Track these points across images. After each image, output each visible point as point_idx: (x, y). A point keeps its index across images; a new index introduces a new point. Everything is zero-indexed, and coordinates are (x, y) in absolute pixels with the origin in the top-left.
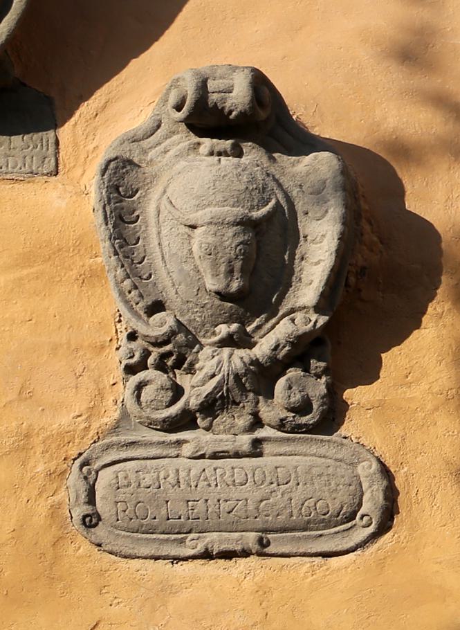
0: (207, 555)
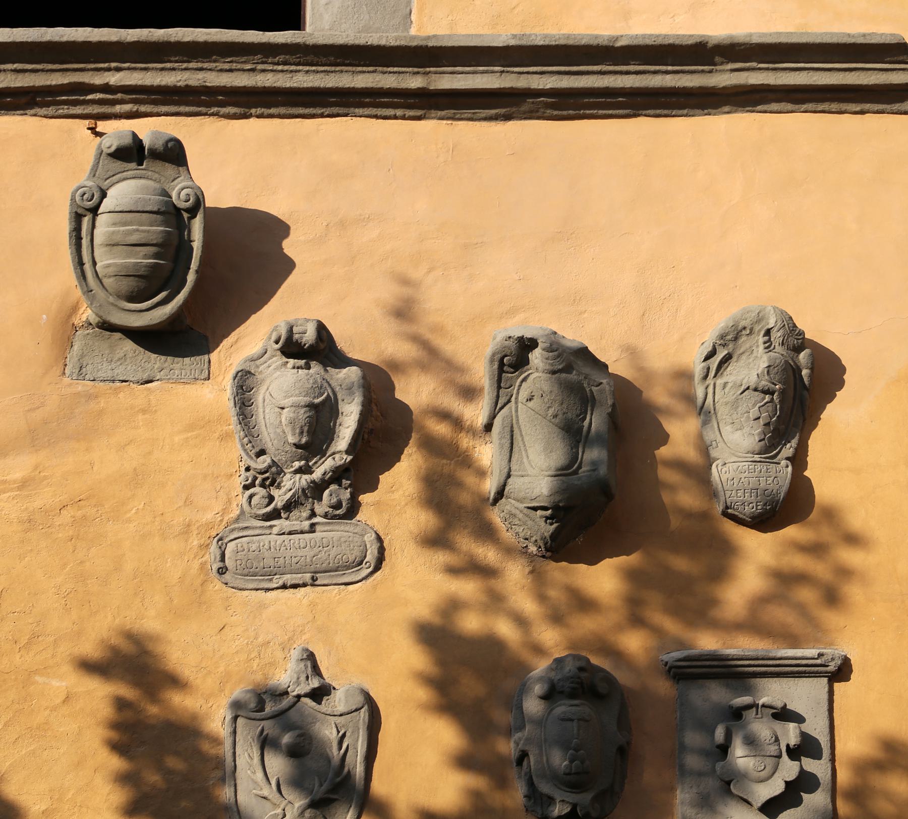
0: (284, 587)
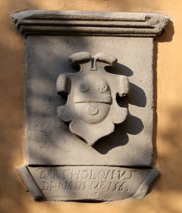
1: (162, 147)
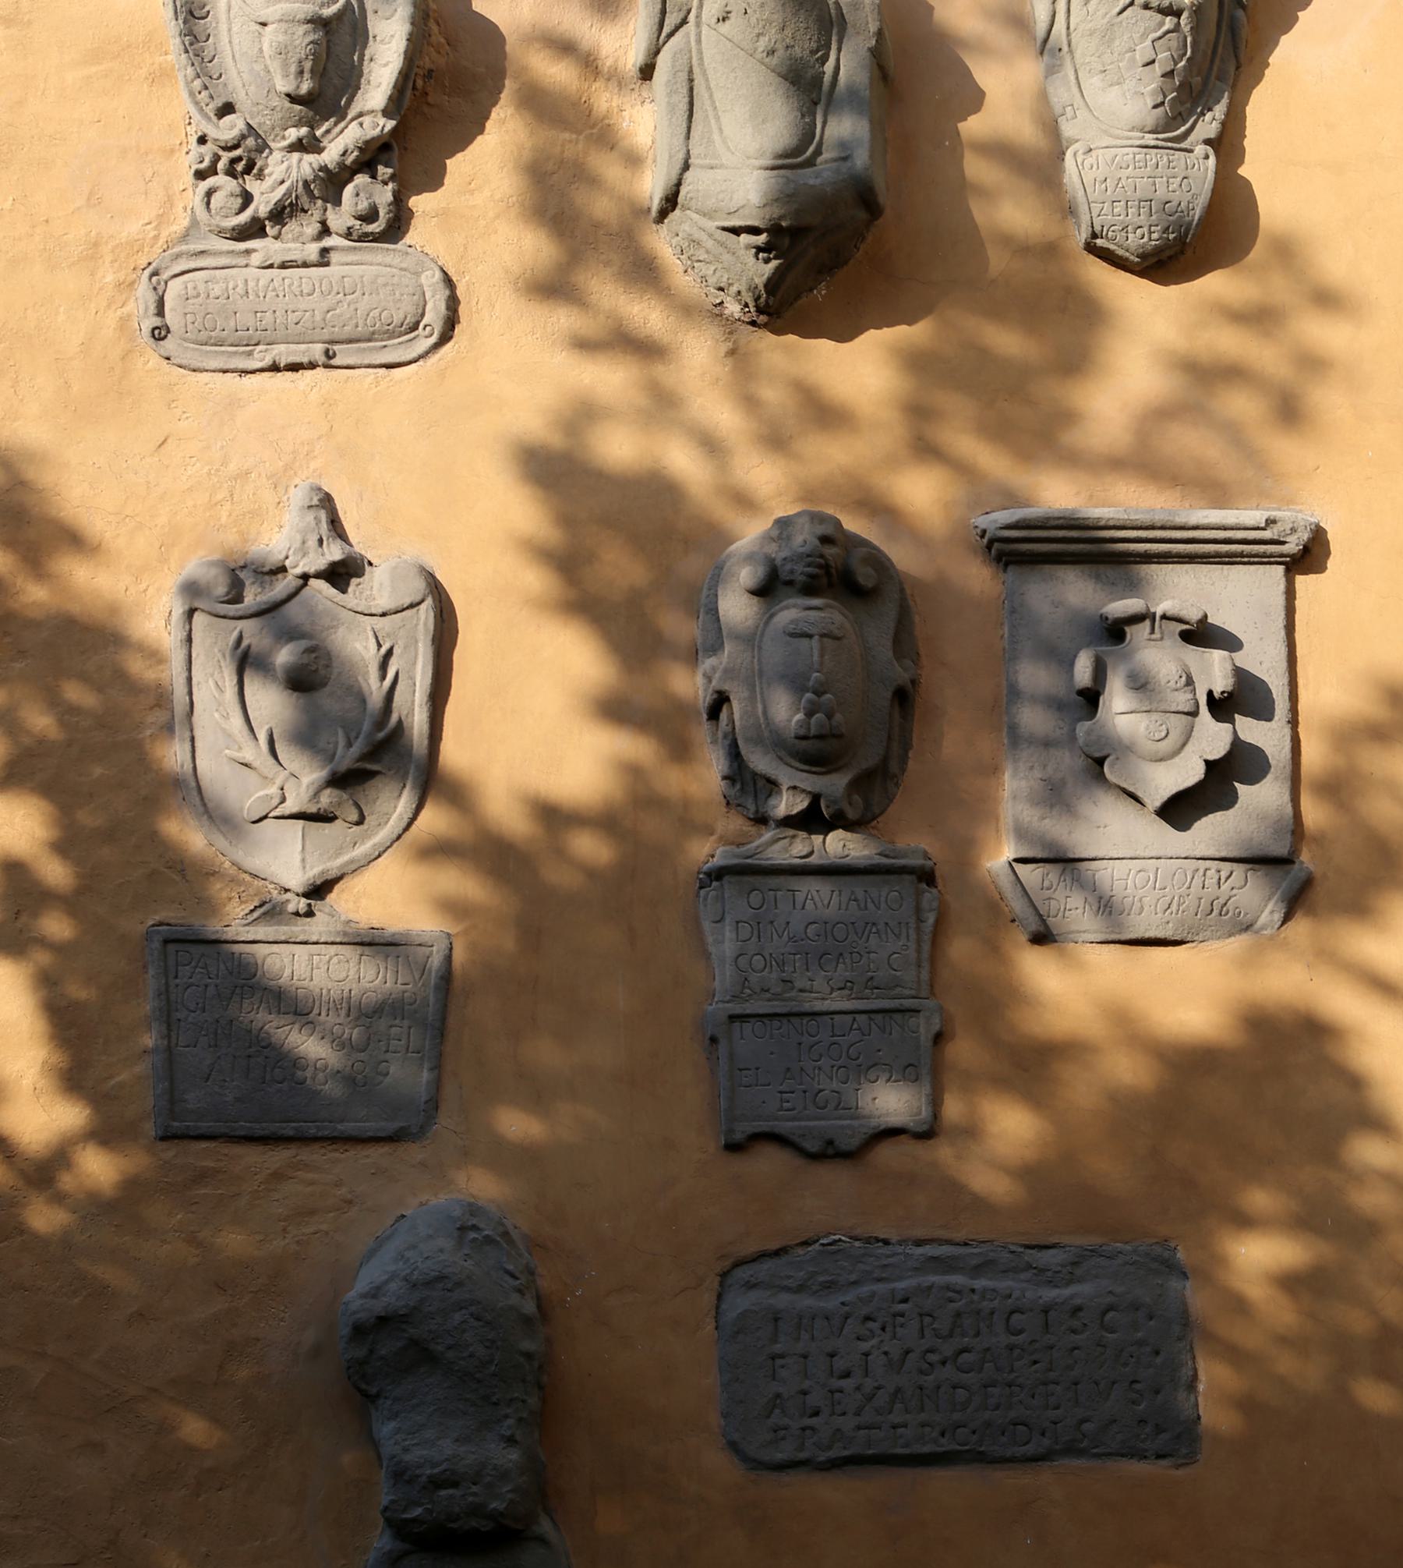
0: (274, 368)
1: (1314, 813)
